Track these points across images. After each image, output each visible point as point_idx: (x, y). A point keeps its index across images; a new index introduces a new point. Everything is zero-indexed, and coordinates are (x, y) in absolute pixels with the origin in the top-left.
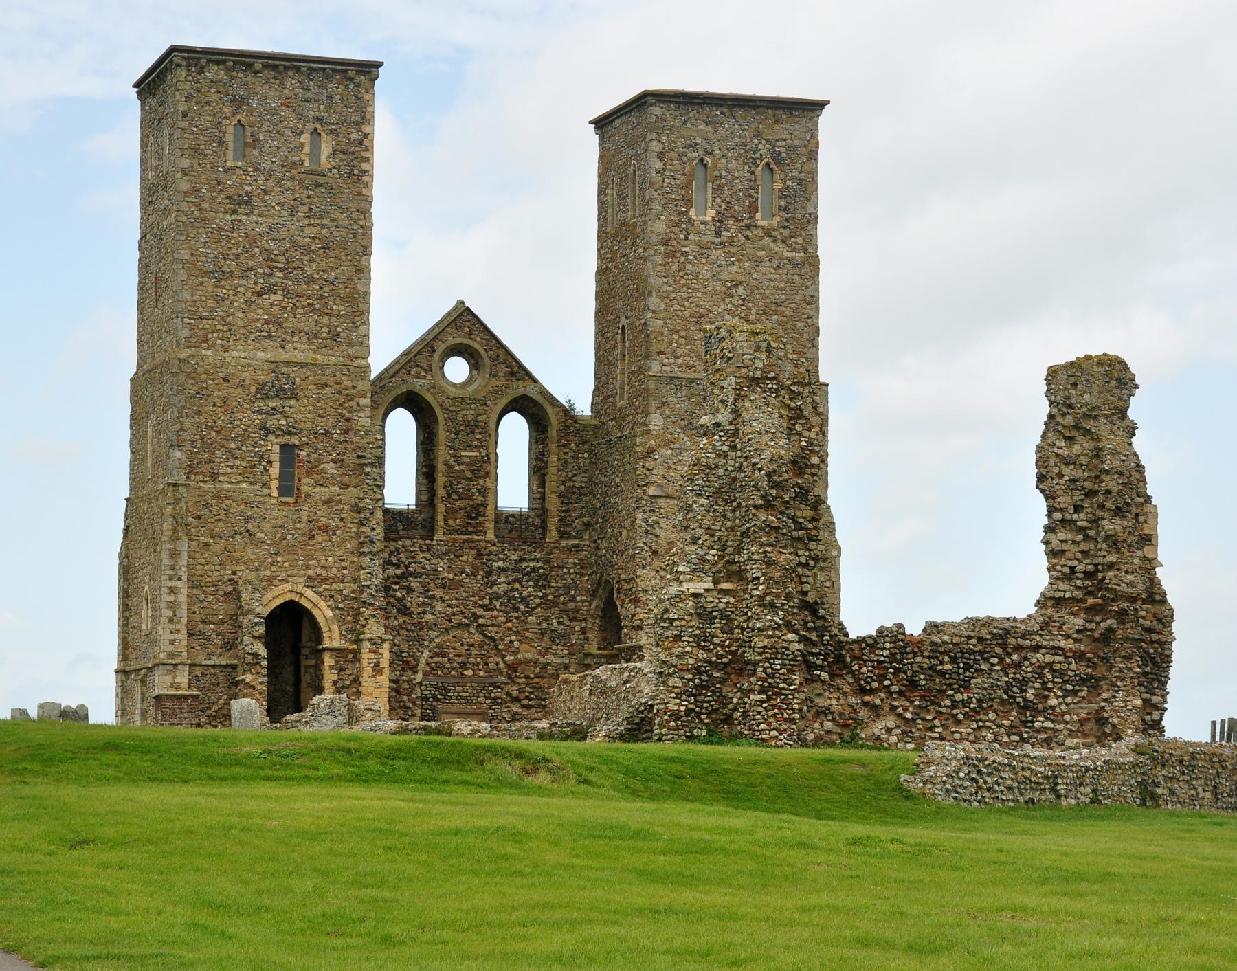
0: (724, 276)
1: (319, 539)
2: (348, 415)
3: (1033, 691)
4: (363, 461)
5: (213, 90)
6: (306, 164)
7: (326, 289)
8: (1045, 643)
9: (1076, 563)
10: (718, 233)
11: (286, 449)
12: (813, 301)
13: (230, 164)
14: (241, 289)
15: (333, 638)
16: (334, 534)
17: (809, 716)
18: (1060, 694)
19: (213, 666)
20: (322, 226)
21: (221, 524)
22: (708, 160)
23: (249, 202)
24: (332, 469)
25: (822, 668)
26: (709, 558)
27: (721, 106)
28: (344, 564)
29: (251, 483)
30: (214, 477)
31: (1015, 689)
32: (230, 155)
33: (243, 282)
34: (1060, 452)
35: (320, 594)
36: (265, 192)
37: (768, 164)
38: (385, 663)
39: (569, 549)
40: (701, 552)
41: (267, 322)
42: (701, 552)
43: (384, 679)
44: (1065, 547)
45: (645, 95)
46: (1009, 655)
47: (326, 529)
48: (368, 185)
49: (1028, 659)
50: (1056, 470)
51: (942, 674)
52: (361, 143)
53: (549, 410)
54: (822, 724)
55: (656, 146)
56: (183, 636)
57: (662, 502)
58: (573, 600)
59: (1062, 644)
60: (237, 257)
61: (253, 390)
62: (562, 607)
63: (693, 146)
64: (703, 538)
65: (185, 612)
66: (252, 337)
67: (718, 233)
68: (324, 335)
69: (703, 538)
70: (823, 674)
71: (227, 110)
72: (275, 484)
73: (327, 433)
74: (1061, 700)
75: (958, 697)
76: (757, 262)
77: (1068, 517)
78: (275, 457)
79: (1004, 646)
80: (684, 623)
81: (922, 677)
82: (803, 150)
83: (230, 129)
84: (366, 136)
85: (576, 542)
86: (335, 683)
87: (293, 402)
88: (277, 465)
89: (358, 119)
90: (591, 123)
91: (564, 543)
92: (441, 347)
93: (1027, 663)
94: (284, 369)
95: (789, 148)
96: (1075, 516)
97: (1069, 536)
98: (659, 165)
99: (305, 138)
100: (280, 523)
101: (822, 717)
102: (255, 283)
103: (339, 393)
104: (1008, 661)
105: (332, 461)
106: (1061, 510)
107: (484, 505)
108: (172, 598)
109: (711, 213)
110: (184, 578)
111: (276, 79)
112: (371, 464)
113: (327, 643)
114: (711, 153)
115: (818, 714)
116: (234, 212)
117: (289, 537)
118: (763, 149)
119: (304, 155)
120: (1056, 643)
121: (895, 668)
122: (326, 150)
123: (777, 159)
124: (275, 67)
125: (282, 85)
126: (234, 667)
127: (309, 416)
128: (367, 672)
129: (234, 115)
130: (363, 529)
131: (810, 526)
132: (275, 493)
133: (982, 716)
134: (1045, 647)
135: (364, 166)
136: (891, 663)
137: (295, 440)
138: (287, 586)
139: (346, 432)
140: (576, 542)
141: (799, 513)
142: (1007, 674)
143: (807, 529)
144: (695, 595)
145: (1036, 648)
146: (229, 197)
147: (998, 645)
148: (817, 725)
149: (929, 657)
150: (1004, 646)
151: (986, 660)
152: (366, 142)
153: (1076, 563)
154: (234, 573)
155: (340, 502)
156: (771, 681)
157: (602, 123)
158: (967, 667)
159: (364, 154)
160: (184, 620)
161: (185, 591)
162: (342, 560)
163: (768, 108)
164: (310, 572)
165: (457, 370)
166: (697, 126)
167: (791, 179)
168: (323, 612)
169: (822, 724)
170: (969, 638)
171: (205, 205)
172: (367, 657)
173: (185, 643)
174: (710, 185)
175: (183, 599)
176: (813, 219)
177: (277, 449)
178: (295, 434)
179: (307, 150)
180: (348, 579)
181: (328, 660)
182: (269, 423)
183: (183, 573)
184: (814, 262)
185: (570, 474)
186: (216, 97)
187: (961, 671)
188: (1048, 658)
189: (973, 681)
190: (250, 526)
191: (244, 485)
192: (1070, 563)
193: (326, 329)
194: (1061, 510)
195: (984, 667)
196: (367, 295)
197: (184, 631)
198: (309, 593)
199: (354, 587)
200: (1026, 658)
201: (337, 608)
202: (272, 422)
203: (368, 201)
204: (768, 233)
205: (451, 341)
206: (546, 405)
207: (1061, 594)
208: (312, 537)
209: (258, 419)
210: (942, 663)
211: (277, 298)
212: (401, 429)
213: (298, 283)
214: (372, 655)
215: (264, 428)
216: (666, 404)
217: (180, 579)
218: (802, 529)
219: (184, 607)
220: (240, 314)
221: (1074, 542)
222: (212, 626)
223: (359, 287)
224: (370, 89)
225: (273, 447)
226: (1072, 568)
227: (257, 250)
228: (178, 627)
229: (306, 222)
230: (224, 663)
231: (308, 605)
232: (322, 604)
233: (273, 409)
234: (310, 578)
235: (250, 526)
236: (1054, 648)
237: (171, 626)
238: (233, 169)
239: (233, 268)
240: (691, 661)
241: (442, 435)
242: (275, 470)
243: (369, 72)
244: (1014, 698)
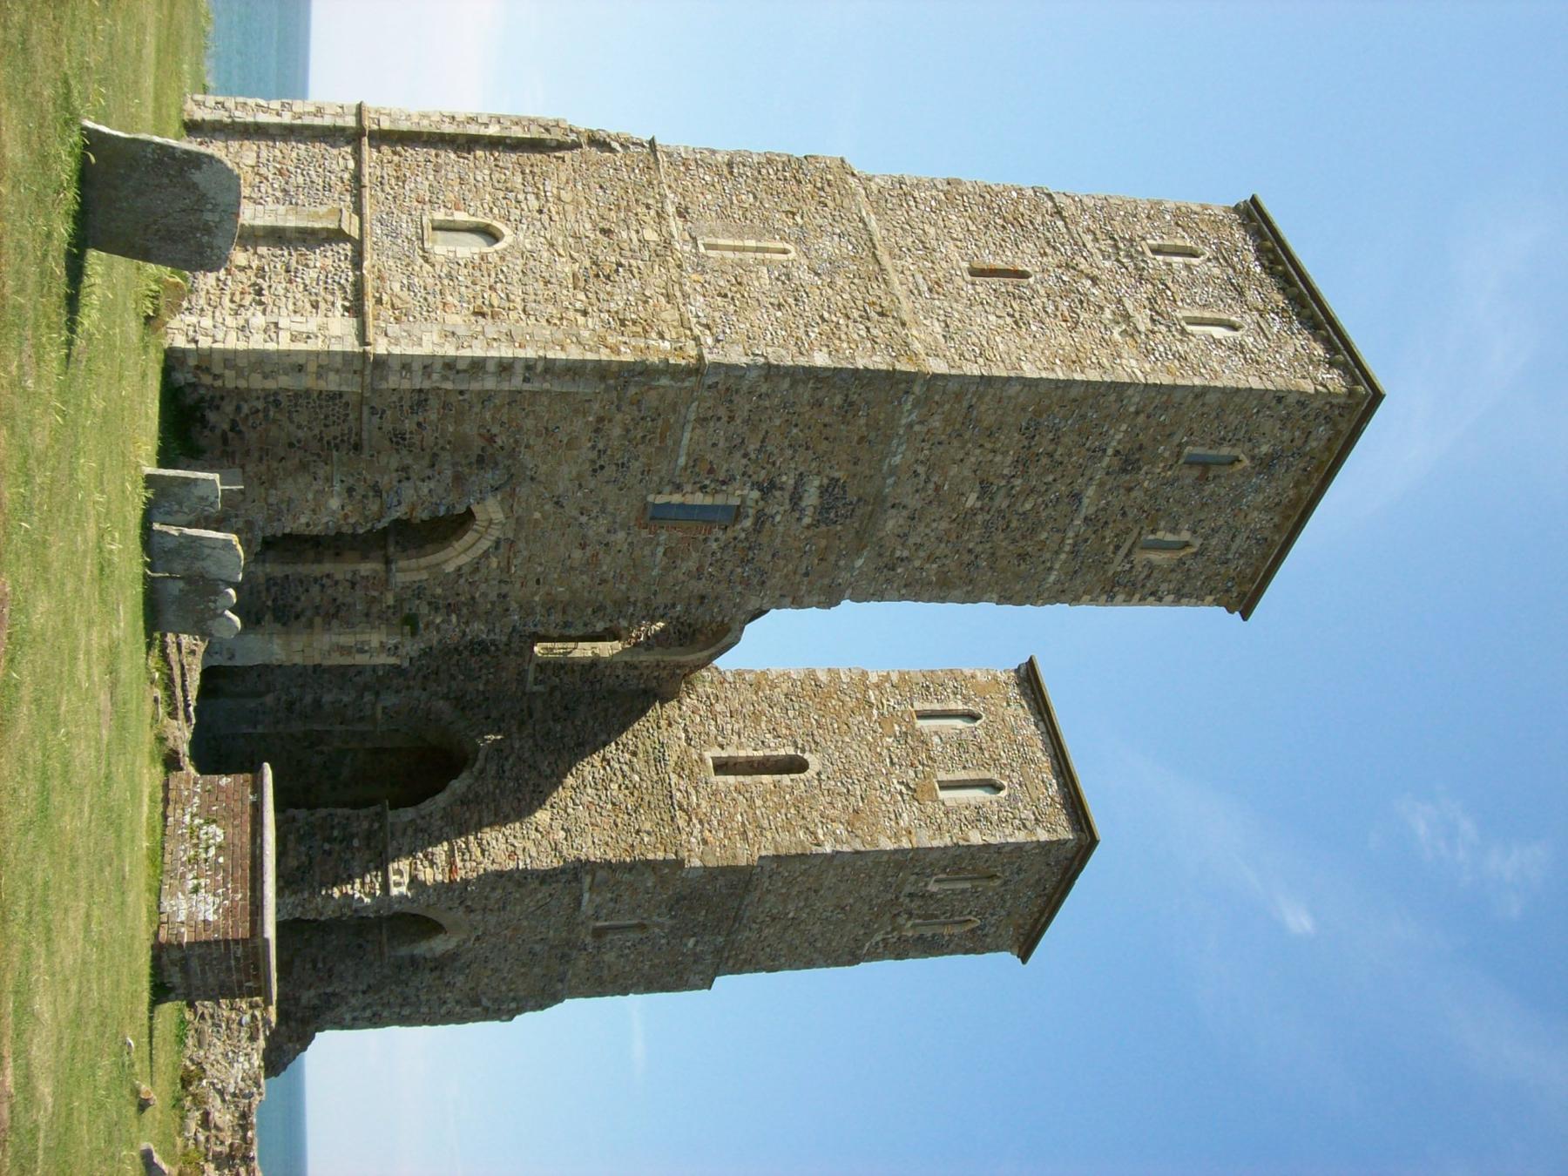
1: (577, 554)
2: (768, 584)
4: (695, 603)
5: (1297, 433)
6: (1151, 537)
7: (967, 558)
10: (911, 895)
11: (737, 513)
12: (810, 964)
13: (1188, 449)
14: (998, 458)
15: (410, 571)
16: (582, 573)
19: (360, 418)
20: (1057, 553)
21: (617, 431)
22: (998, 882)
23: (1124, 471)
24: (691, 565)
27: (1055, 889)
28: (532, 583)
29: (685, 468)
30: (702, 421)
32: (1199, 450)
33: (1009, 460)
35: (486, 554)
36: (1130, 490)
38: (361, 659)
39: (521, 677)
41: (938, 488)
43: (337, 660)
45: (1093, 842)
47: (594, 561)
48: (1094, 601)
52: (1152, 594)
53: (706, 653)
56: (419, 382)
57: (587, 880)
58: (453, 677)
60: (1050, 455)
61: (836, 475)
62: (444, 667)
65: (463, 387)
66: (921, 469)
68: (898, 554)
71: (1265, 449)
72: (676, 498)
73: (744, 562)
78: (720, 500)
83: (1237, 452)
84: (1160, 600)
85: (531, 678)
86: (328, 576)
87: (807, 521)
88: (708, 501)
89: (1186, 590)
90: (1031, 664)
91: (532, 667)
94: (859, 512)
99: (1185, 536)
100: (610, 508)
102: (1003, 476)
103: (807, 574)
105: (700, 569)
108: (491, 367)
109: (933, 887)
110: (527, 387)
111: (1277, 504)
112: (687, 611)
113: (403, 564)
116: (1117, 453)
117: (584, 519)
118: (993, 920)
119: (1160, 535)
122: (1156, 557)
124: (1293, 505)
125: (1267, 509)
126: (357, 447)
127: (778, 541)
128: (347, 640)
129: (1253, 458)
130: (590, 610)
132: (661, 500)
135: (1120, 597)
137: (748, 523)
138: (499, 516)
139: (746, 583)
140: (531, 678)
146: (1141, 448)
152: (1152, 599)
154: (528, 446)
155: (635, 578)
157: (1029, 680)
159: (1137, 596)
160: (449, 386)
161: (506, 386)
162: (538, 582)
163: (1037, 920)
164: (521, 545)
167: (950, 941)
168: (457, 556)
171: (1142, 417)
172: (375, 639)
173: (406, 385)
174: (968, 885)
175: (490, 384)
176: (899, 957)
177: (735, 501)
178: (755, 524)
179: (1170, 537)
180: (505, 589)
181: (366, 568)
182: (778, 493)
183: (535, 386)
184: (854, 960)
185: (619, 672)
186: (1286, 435)
190: (610, 471)
191: (682, 461)
193: (906, 554)
196: (943, 600)
197: (426, 385)
198: (486, 544)
199: (493, 596)
201: (460, 576)
202: (781, 498)
203: (1075, 600)
206: (712, 650)
208: (583, 546)
209: (788, 480)
211: (972, 500)
213: (986, 525)
214: (375, 643)
215: (773, 485)
217: (526, 380)
219: (475, 386)
220: (960, 455)
222: (433, 416)
223: (957, 593)
224: (1218, 603)
225: (741, 494)
227: (1050, 478)
228: (435, 376)
229: (1071, 534)
230: (365, 435)
231: (469, 537)
232: (464, 559)
233: (800, 498)
234: (512, 543)
235: (610, 471)
237: (438, 366)
238: (1179, 455)
239: (1035, 449)
242: (699, 499)
243: (1240, 602)
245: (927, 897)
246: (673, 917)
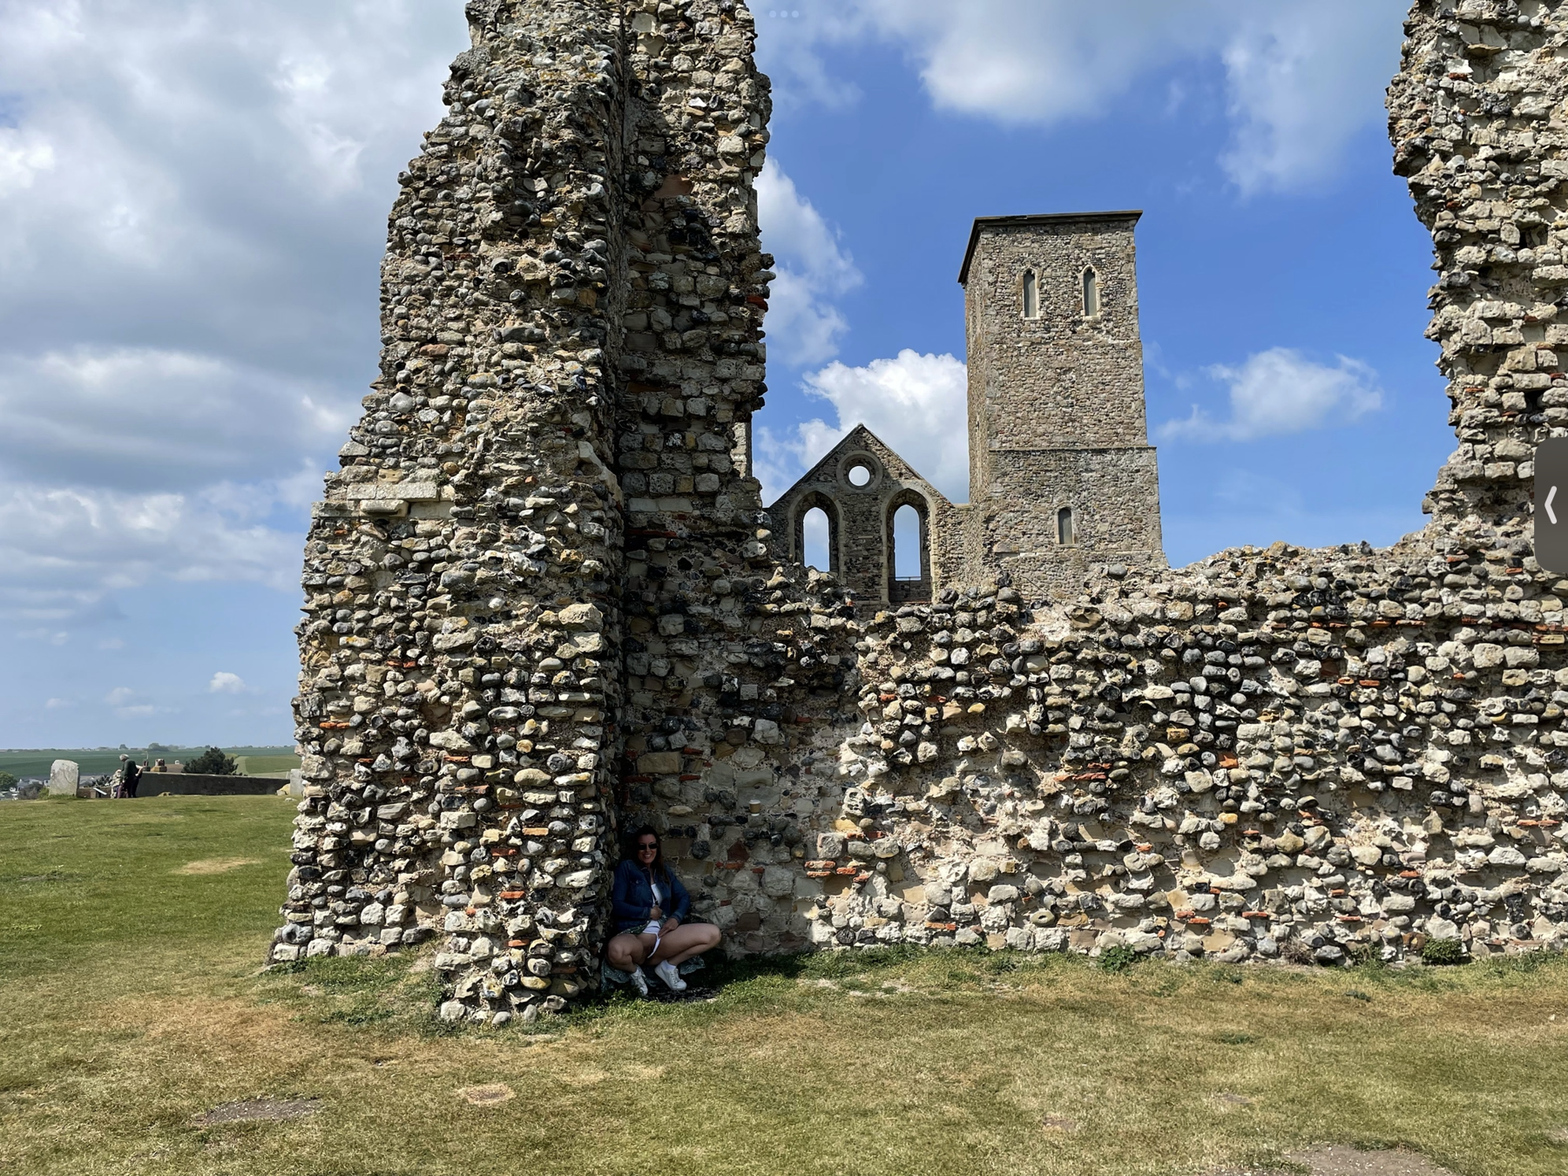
0: (1056, 364)
3: (1444, 755)
8: (1468, 609)
9: (1542, 379)
17: (720, 854)
18: (1533, 756)
22: (1035, 271)
25: (758, 708)
26: (429, 415)
31: (1385, 751)
34: (1462, 86)
37: (1089, 270)
40: (401, 401)
42: (401, 401)
44: (1500, 335)
46: (1360, 649)
49: (1420, 661)
50: (1454, 133)
51: (1142, 711)
54: (760, 873)
55: (988, 264)
59: (1527, 610)
63: (1021, 261)
64: (411, 365)
67: (1048, 330)
69: (411, 365)
70: (761, 724)
74: (1538, 780)
75: (1197, 781)
76: (1084, 351)
77: (1503, 254)
79: (1337, 622)
80: (339, 597)
81: (1076, 721)
82: (1121, 255)
92: (843, 459)
93: (1414, 672)
95: (1107, 254)
96: (1524, 254)
97: (1511, 309)
98: (991, 279)
101: (763, 854)
104: (1353, 664)
106: (1480, 238)
107: (879, 576)
109: (1038, 315)
114: (1037, 265)
115: (740, 853)
120: (1503, 610)
121: (990, 702)
123: (1098, 263)
131: (718, 316)
133: (1286, 839)
134: (1471, 622)
136: (981, 682)
141: (684, 283)
142: (1354, 706)
143: (708, 322)
144: (381, 518)
145: (1444, 627)
147: (1322, 621)
148: (743, 878)
149: (1097, 665)
150: (1337, 622)
151: (1286, 666)
153: (1542, 379)
156: (482, 761)
158: (1224, 689)
165: (859, 476)
166: (1025, 245)
169: (760, 873)
170: (1219, 604)
187: (1201, 701)
188: (1483, 656)
189: (1243, 730)
192: (1524, 380)
194: (1480, 238)
195: (1280, 684)
200: (1413, 658)
204: (1094, 326)
205: (851, 453)
207: (1506, 469)
210: (1139, 679)
212: (816, 522)
216: (1005, 474)
218: (696, 323)
221: (1534, 326)
226: (1533, 395)
236: (1499, 622)
240: (361, 703)
241: (842, 524)
244: (1386, 778)
245: (1049, 317)
246: (1054, 493)
